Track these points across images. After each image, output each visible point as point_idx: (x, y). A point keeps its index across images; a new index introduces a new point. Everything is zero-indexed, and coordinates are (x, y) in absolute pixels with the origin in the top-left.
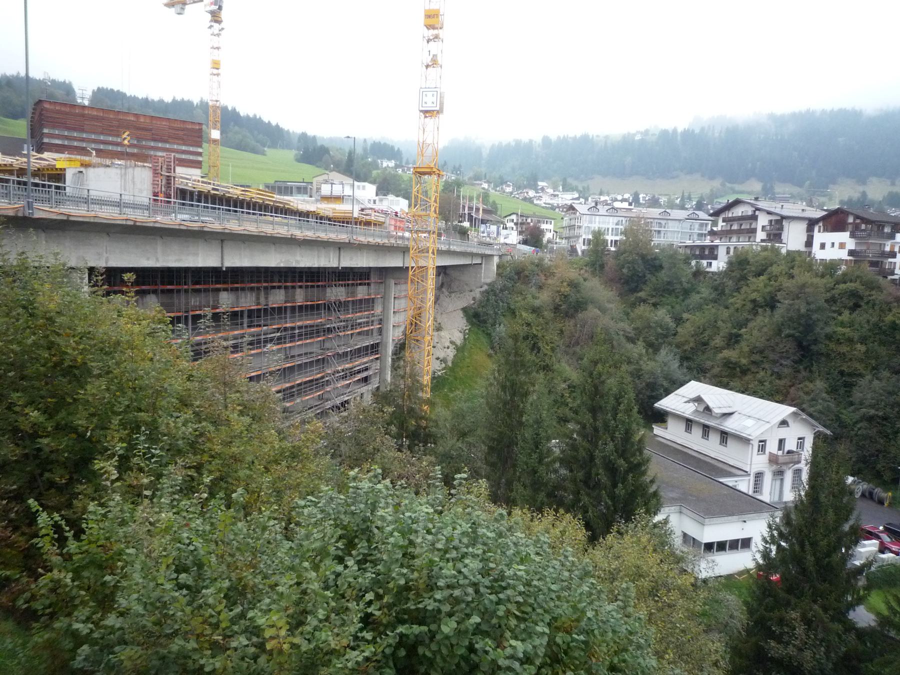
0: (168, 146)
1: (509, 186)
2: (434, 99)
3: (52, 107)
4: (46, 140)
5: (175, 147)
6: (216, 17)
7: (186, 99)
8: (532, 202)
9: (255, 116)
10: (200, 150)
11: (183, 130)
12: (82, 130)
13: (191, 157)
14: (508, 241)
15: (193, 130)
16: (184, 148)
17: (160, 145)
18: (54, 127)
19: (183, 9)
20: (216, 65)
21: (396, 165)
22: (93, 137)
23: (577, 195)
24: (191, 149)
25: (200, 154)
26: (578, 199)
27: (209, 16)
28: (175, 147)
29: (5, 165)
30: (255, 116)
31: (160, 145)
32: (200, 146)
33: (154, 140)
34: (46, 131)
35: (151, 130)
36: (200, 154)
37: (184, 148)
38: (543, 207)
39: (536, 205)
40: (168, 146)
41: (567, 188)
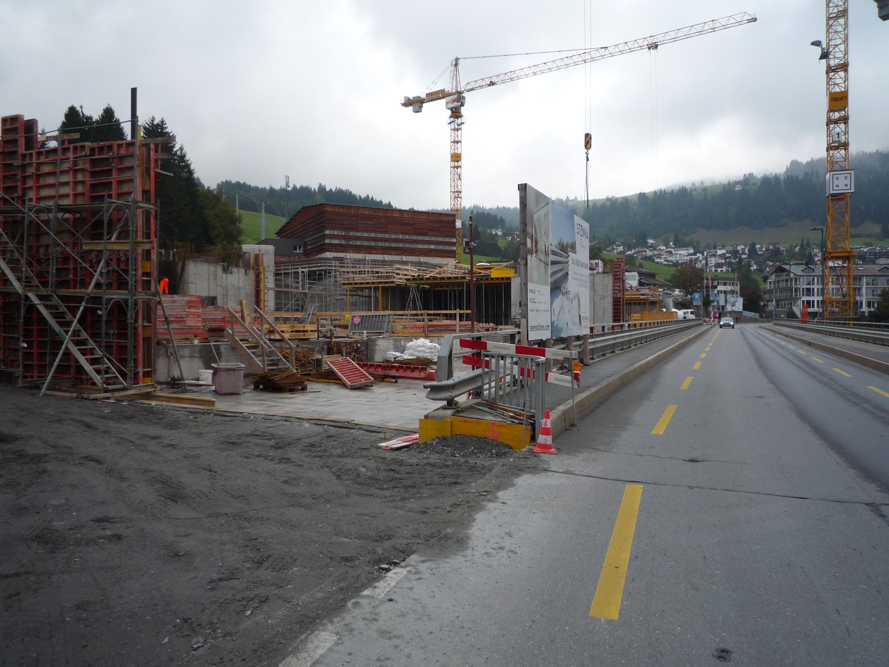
0: (427, 238)
2: (848, 182)
4: (327, 241)
5: (433, 239)
6: (456, 113)
7: (305, 185)
8: (653, 261)
9: (368, 196)
10: (454, 240)
11: (440, 222)
12: (357, 230)
13: (447, 248)
14: (736, 309)
15: (448, 222)
16: (440, 239)
17: (420, 238)
18: (334, 229)
19: (421, 107)
20: (456, 157)
21: (504, 233)
22: (365, 235)
23: (692, 251)
24: (446, 240)
25: (454, 244)
26: (694, 254)
27: (449, 113)
28: (433, 239)
29: (455, 278)
30: (368, 196)
31: (420, 238)
32: (454, 237)
33: (415, 234)
34: (327, 232)
36: (454, 244)
37: (440, 239)
38: (665, 265)
39: (658, 263)
40: (427, 238)
41: (679, 244)
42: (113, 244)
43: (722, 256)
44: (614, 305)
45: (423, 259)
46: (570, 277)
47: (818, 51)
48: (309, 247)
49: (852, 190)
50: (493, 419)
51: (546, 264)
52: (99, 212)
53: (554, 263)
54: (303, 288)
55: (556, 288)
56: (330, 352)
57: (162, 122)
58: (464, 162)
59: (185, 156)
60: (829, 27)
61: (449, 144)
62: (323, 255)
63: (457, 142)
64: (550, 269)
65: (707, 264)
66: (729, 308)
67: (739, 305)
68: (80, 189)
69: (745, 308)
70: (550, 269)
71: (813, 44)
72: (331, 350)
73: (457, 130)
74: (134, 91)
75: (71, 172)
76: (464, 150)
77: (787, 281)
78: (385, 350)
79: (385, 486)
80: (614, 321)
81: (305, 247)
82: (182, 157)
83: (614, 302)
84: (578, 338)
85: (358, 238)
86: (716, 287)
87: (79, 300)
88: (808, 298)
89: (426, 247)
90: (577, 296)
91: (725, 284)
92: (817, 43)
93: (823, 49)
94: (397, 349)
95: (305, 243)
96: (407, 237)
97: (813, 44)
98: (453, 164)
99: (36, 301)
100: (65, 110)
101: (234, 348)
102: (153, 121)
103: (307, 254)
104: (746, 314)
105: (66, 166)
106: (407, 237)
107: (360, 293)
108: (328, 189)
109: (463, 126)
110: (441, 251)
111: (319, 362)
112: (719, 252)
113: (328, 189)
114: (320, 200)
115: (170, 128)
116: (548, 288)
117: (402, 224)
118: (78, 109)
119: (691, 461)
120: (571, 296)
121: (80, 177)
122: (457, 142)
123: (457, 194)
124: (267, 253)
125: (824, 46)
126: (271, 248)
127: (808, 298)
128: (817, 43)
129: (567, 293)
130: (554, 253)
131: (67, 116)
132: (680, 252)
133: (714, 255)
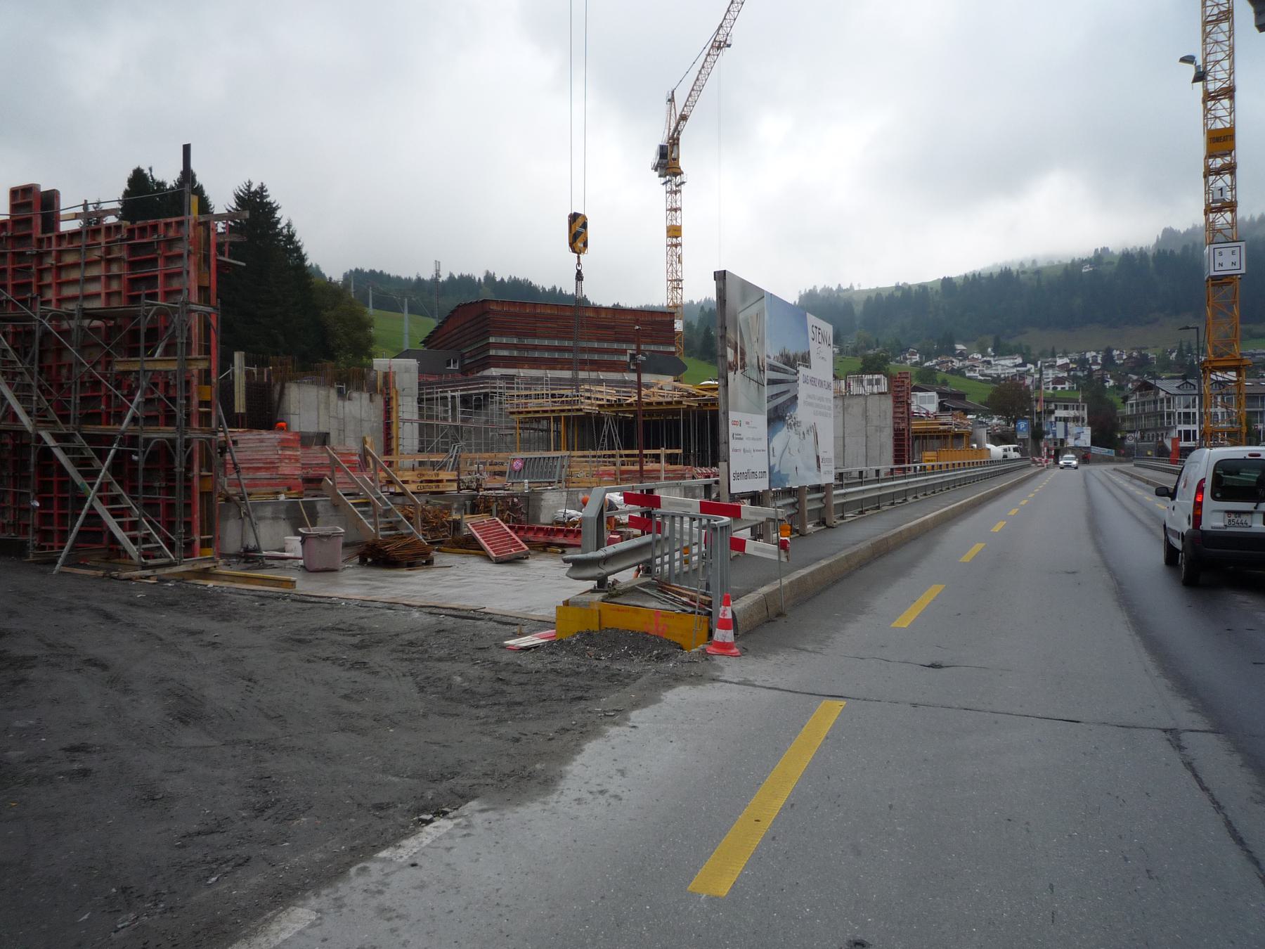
1: (913, 354)
2: (1236, 258)
3: (499, 308)
4: (492, 352)
7: (465, 273)
8: (963, 375)
9: (554, 288)
12: (535, 336)
14: (1080, 443)
22: (546, 342)
23: (1019, 361)
26: (1023, 365)
29: (669, 403)
30: (554, 288)
32: (672, 344)
34: (492, 340)
35: (613, 327)
39: (970, 378)
41: (1001, 351)
42: (158, 362)
43: (1064, 367)
44: (895, 440)
46: (799, 401)
47: (1190, 70)
48: (467, 362)
49: (1243, 271)
50: (659, 606)
51: (760, 384)
52: (134, 318)
53: (772, 382)
54: (454, 419)
55: (777, 418)
56: (474, 509)
57: (262, 188)
58: (685, 238)
59: (293, 235)
60: (1206, 35)
61: (662, 213)
62: (486, 373)
63: (676, 210)
64: (767, 391)
65: (1040, 380)
66: (1071, 442)
67: (1085, 438)
68: (115, 286)
69: (1094, 442)
70: (767, 391)
71: (1183, 60)
72: (476, 506)
73: (676, 192)
74: (187, 149)
75: (103, 264)
76: (686, 221)
77: (1155, 402)
78: (555, 506)
79: (483, 703)
80: (896, 462)
81: (462, 361)
82: (290, 237)
83: (896, 435)
84: (818, 489)
85: (535, 348)
86: (1052, 412)
87: (109, 440)
88: (1187, 427)
90: (813, 429)
91: (1066, 408)
92: (1188, 59)
93: (1197, 67)
94: (571, 504)
95: (462, 355)
96: (605, 345)
97: (1183, 60)
98: (670, 241)
99: (51, 442)
100: (128, 173)
101: (336, 506)
102: (249, 186)
103: (465, 371)
104: (1096, 450)
105: (96, 254)
106: (605, 345)
107: (535, 425)
108: (498, 279)
111: (457, 525)
112: (1060, 362)
113: (498, 279)
114: (487, 294)
115: (273, 197)
116: (763, 419)
118: (146, 171)
119: (933, 666)
120: (803, 428)
121: (115, 269)
122: (676, 210)
123: (676, 283)
124: (407, 370)
125: (1199, 62)
126: (413, 363)
127: (1187, 427)
128: (1188, 59)
129: (796, 424)
130: (773, 368)
131: (131, 182)
132: (1002, 362)
133: (1052, 367)
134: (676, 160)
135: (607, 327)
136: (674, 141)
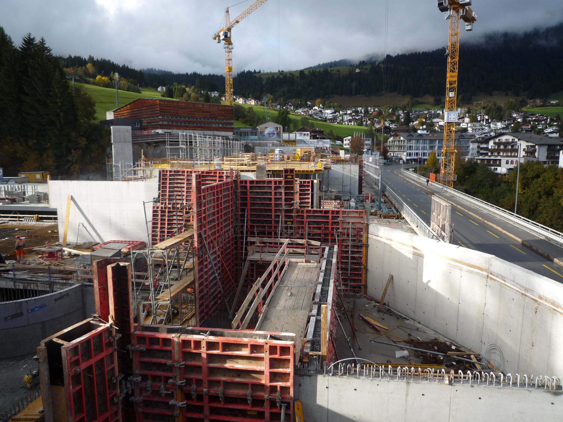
1: (290, 106)
2: (455, 117)
7: (77, 55)
9: (124, 65)
10: (232, 121)
23: (333, 111)
26: (335, 113)
30: (124, 65)
39: (315, 119)
43: (350, 114)
45: (216, 133)
57: (42, 40)
63: (229, 60)
65: (343, 119)
73: (229, 52)
88: (410, 151)
89: (217, 125)
102: (30, 36)
108: (95, 59)
109: (233, 50)
110: (225, 128)
112: (349, 112)
117: (203, 112)
124: (127, 131)
126: (129, 128)
127: (410, 151)
132: (327, 111)
133: (346, 114)
134: (230, 38)
135: (207, 112)
136: (229, 30)
